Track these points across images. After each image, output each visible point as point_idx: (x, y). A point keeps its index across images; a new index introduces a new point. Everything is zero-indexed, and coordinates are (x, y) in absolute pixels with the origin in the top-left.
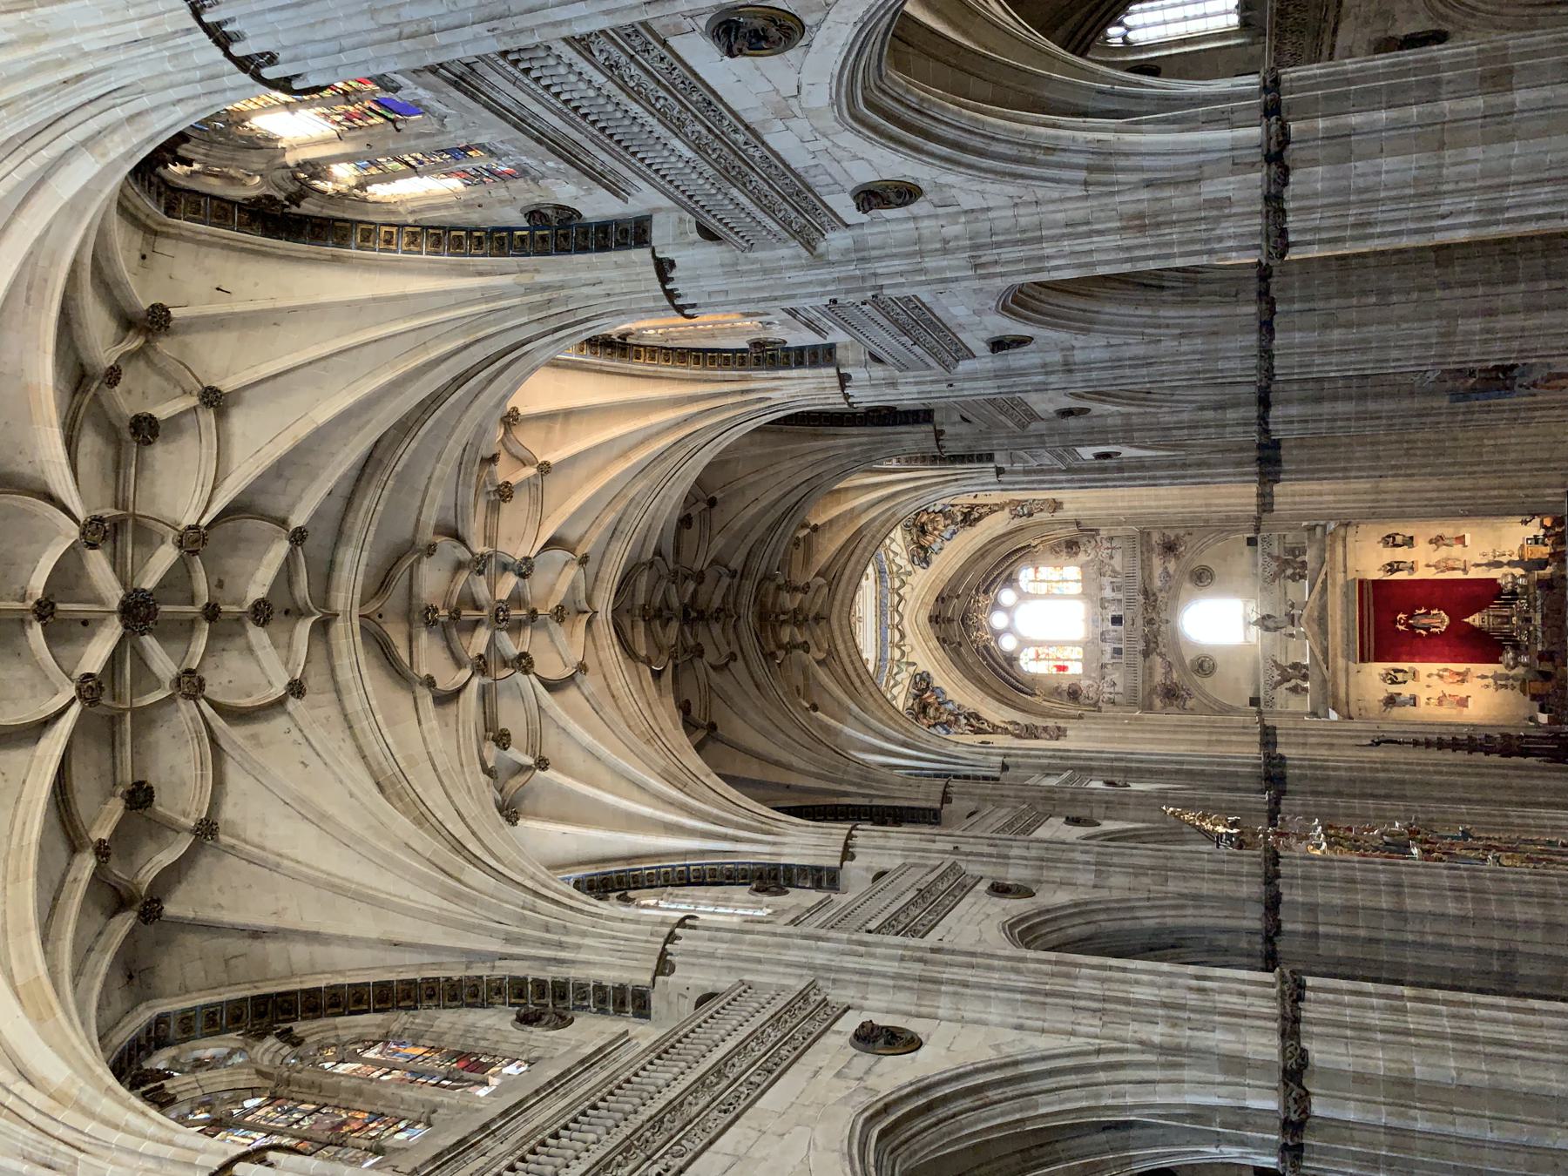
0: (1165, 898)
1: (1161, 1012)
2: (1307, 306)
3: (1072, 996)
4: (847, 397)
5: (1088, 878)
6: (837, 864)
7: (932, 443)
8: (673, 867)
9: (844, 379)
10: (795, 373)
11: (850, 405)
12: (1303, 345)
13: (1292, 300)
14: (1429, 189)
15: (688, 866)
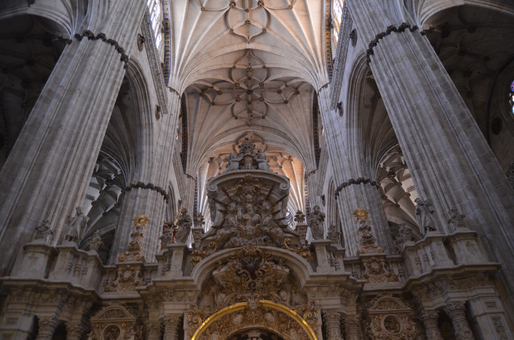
0: (152, 158)
1: (119, 22)
2: (363, 191)
3: (126, 10)
4: (320, 90)
5: (161, 142)
6: (169, 85)
7: (310, 171)
8: (170, 48)
9: (326, 86)
10: (327, 75)
11: (318, 94)
12: (349, 194)
13: (365, 188)
14: (394, 61)
15: (170, 52)
